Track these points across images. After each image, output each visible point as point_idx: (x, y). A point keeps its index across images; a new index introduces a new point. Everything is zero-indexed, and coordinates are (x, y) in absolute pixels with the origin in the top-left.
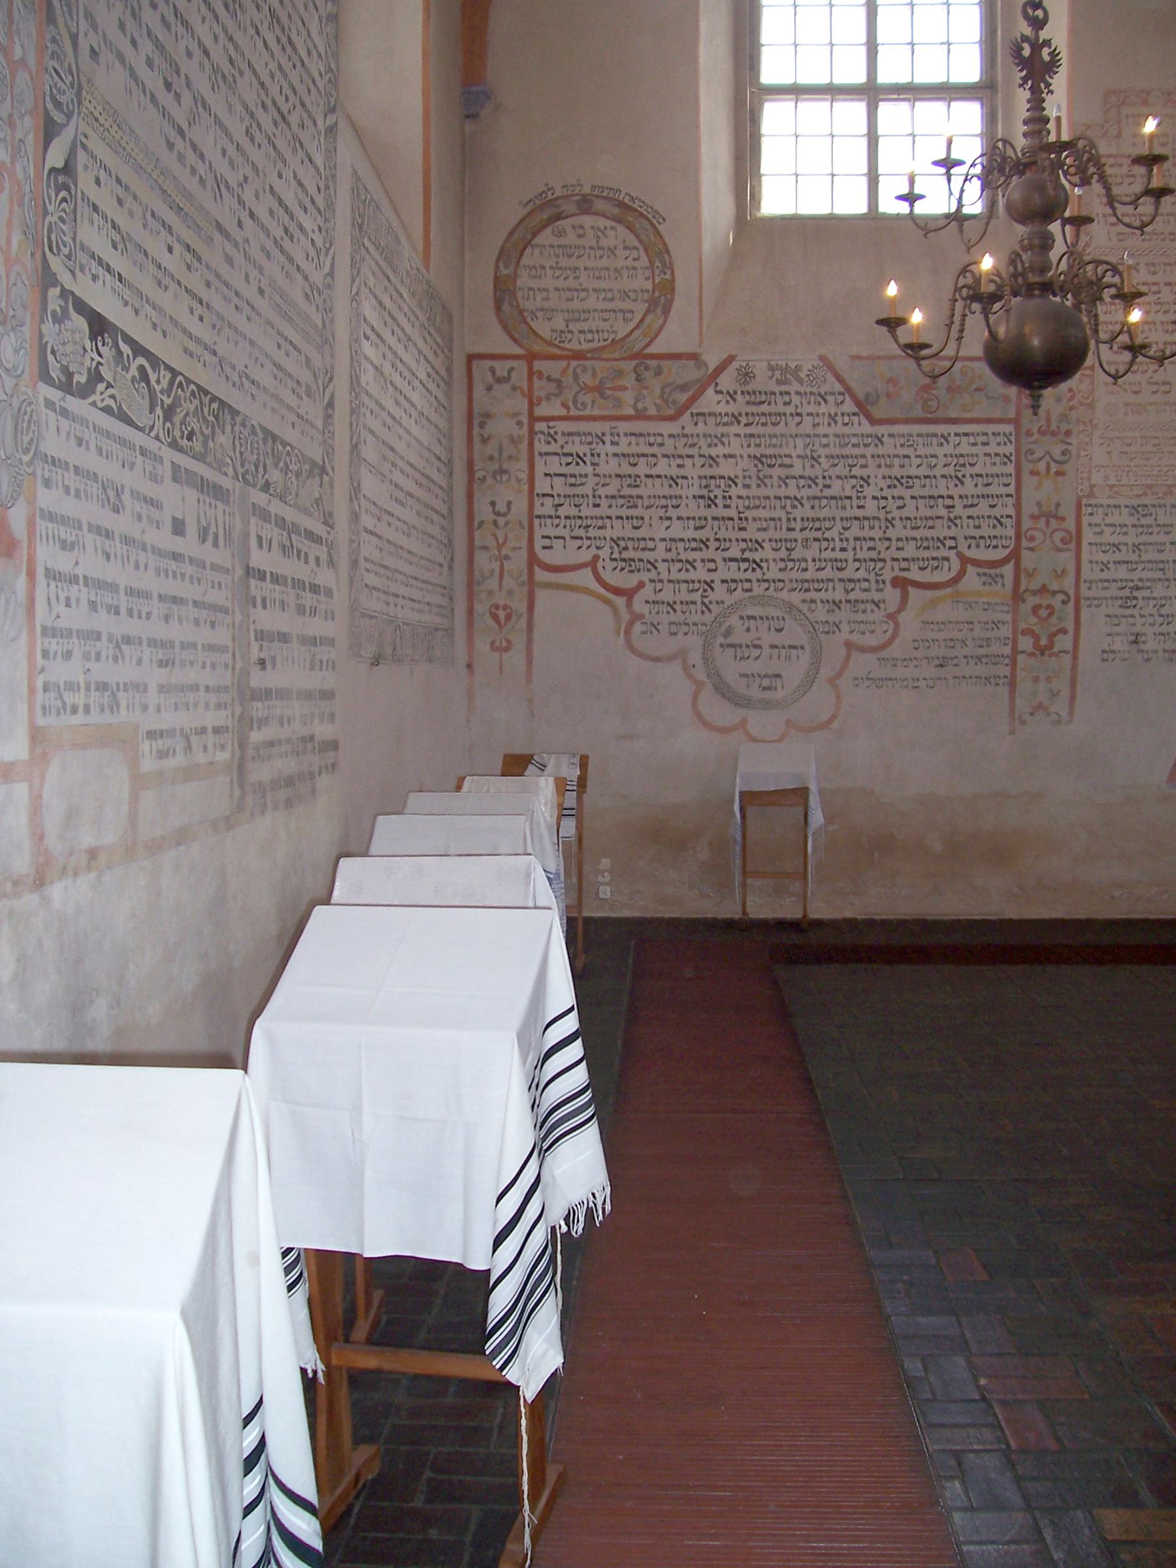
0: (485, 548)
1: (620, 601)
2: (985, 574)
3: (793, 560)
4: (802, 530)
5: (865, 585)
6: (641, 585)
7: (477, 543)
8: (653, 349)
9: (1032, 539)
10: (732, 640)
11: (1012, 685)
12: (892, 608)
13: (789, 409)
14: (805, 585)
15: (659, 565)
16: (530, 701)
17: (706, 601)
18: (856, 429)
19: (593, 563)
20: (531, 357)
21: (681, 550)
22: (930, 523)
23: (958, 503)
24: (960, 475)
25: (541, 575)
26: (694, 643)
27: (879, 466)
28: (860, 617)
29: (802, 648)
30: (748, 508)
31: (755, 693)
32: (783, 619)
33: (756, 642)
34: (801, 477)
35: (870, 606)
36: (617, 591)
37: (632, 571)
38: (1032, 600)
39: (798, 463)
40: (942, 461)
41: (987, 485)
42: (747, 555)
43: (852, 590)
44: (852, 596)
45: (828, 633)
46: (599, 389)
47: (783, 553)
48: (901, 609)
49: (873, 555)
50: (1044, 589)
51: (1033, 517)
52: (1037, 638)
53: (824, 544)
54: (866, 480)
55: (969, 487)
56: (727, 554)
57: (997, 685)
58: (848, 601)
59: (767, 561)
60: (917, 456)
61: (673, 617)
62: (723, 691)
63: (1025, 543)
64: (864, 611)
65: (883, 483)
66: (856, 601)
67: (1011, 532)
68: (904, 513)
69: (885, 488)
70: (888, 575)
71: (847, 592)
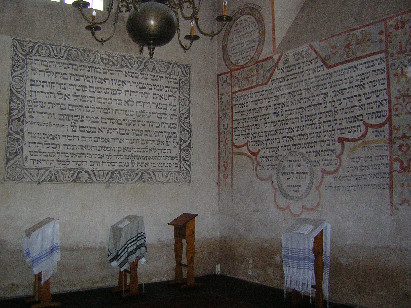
0: (222, 141)
1: (254, 157)
2: (376, 131)
3: (303, 135)
4: (306, 121)
5: (328, 143)
6: (259, 150)
7: (221, 140)
8: (260, 59)
9: (397, 109)
10: (285, 171)
11: (391, 187)
12: (338, 153)
13: (301, 70)
14: (308, 145)
15: (265, 142)
16: (232, 196)
17: (277, 155)
18: (323, 73)
19: (246, 144)
20: (232, 71)
21: (270, 135)
22: (352, 110)
23: (363, 97)
24: (362, 83)
25: (235, 150)
26: (274, 172)
27: (331, 87)
28: (327, 158)
29: (307, 173)
30: (288, 115)
31: (292, 194)
32: (301, 161)
33: (292, 171)
34: (305, 98)
35: (330, 152)
36: (253, 154)
37: (257, 146)
38: (399, 142)
39: (303, 92)
40: (355, 78)
41: (375, 86)
42: (289, 135)
43: (324, 145)
44: (324, 148)
45: (315, 166)
46: (247, 78)
47: (300, 133)
48: (342, 153)
49: (330, 128)
50: (404, 136)
51: (397, 98)
52: (402, 163)
53: (313, 126)
54: (326, 94)
55: (367, 90)
56: (283, 135)
57: (384, 188)
58: (322, 151)
59: (295, 136)
60: (345, 79)
61: (269, 163)
62: (283, 193)
63: (393, 113)
64: (328, 155)
65: (333, 95)
66: (325, 151)
67: (386, 108)
68: (341, 107)
69: (334, 96)
70: (336, 138)
71: (322, 146)
